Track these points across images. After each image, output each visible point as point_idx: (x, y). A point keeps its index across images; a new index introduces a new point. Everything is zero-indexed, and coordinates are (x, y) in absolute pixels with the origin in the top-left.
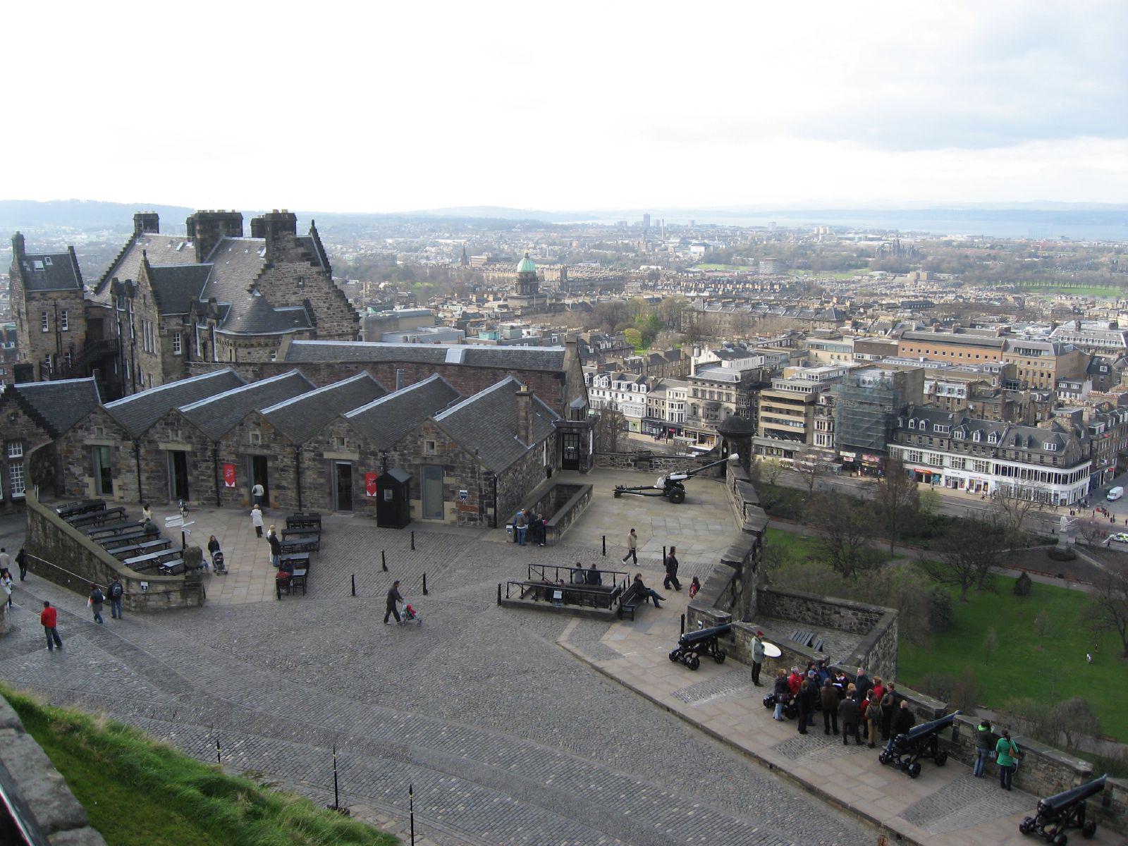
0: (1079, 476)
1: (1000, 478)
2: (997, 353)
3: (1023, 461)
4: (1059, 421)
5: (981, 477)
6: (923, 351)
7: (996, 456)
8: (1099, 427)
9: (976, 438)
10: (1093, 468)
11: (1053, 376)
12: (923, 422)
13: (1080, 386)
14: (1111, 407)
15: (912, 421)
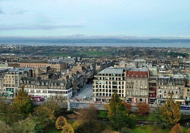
0: (70, 91)
1: (50, 94)
2: (45, 64)
3: (55, 89)
4: (63, 78)
5: (45, 94)
6: (27, 65)
7: (48, 88)
8: (73, 79)
9: (43, 84)
10: (73, 89)
11: (60, 69)
12: (28, 81)
13: (66, 71)
14: (75, 74)
15: (25, 81)
